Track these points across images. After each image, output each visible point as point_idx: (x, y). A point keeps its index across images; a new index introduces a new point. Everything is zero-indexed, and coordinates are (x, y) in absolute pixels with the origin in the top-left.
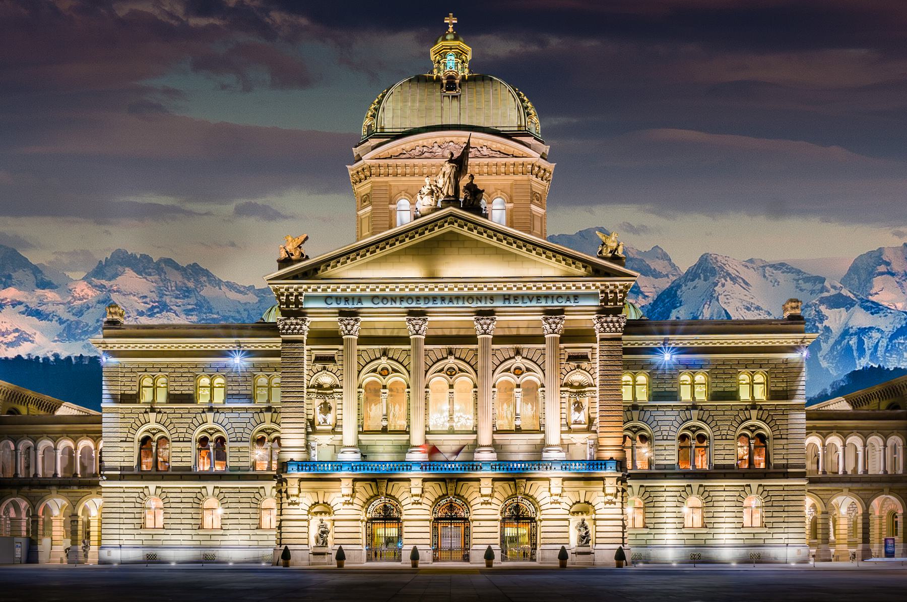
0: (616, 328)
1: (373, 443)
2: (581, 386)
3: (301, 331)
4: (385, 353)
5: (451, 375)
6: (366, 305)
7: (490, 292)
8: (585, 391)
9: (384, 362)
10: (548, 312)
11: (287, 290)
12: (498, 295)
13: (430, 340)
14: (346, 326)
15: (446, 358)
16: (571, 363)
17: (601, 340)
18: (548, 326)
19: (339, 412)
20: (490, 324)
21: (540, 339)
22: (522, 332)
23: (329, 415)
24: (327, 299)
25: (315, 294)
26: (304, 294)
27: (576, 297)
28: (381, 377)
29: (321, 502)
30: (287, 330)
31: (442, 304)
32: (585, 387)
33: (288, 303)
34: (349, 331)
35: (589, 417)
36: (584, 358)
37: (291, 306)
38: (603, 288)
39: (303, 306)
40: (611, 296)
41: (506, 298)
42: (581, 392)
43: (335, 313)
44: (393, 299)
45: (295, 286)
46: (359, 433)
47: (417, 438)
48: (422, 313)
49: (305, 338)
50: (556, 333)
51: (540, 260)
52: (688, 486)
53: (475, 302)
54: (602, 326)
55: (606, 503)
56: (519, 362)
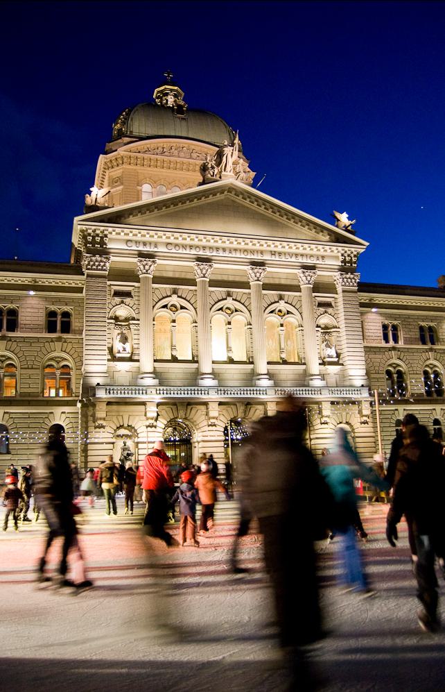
1: (166, 370)
2: (326, 328)
3: (104, 268)
4: (175, 292)
5: (229, 315)
8: (330, 332)
9: (174, 300)
10: (306, 267)
11: (94, 231)
12: (266, 251)
14: (144, 266)
15: (226, 299)
16: (320, 309)
17: (344, 291)
18: (304, 278)
19: (136, 341)
21: (297, 288)
22: (283, 282)
25: (118, 237)
27: (323, 257)
28: (172, 313)
29: (125, 425)
30: (92, 266)
32: (329, 329)
33: (94, 242)
34: (147, 271)
35: (337, 353)
36: (329, 305)
38: (343, 252)
39: (108, 247)
40: (348, 259)
41: (273, 253)
42: (327, 332)
43: (135, 254)
44: (184, 247)
45: (102, 228)
46: (155, 361)
47: (206, 367)
48: (207, 260)
51: (296, 228)
53: (249, 254)
54: (343, 281)
55: (361, 423)
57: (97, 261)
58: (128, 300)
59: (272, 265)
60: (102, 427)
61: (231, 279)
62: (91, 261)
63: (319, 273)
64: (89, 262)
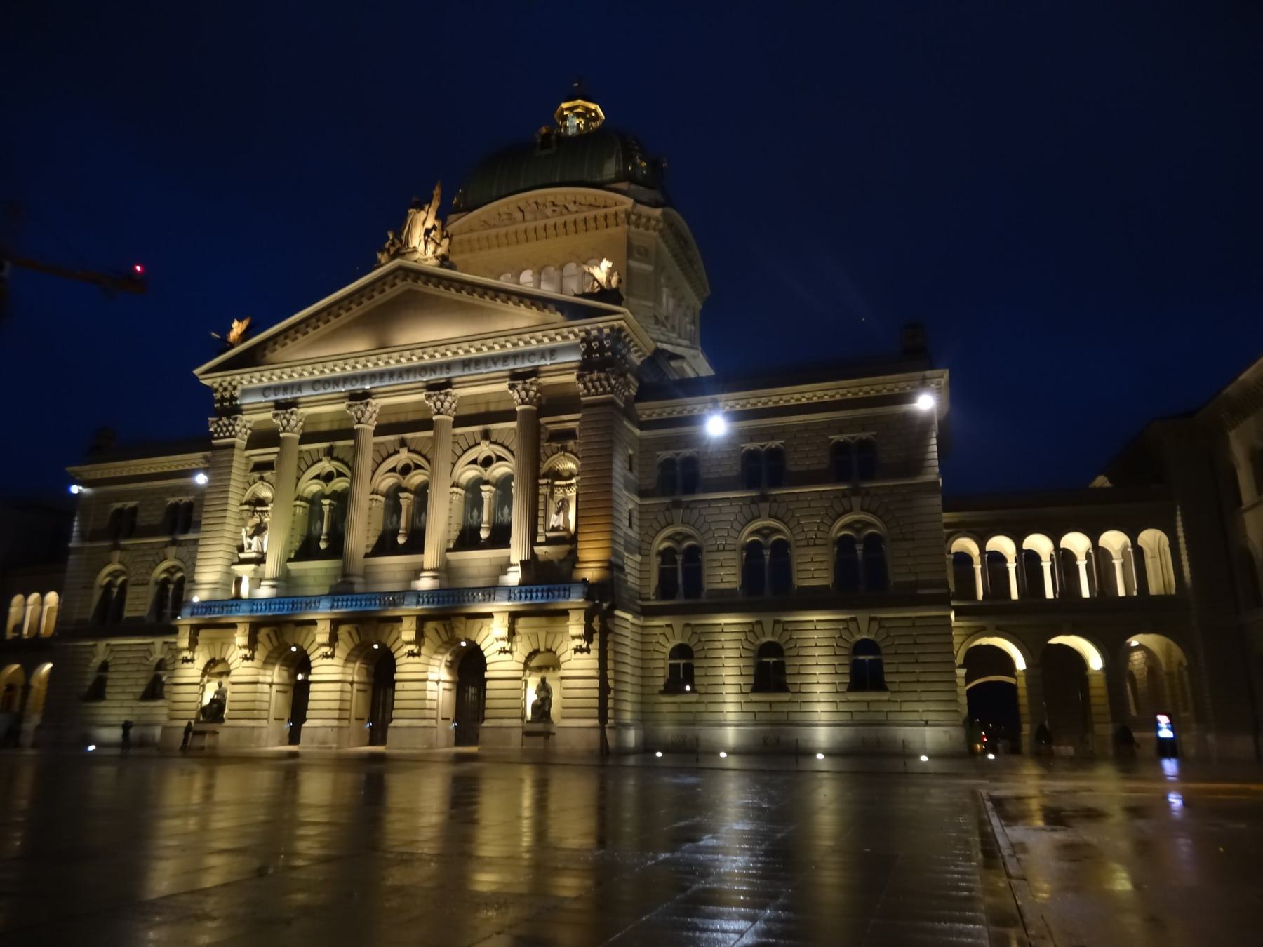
0: (605, 389)
3: (233, 433)
6: (307, 392)
7: (444, 359)
10: (515, 376)
11: (221, 385)
13: (381, 430)
20: (444, 401)
21: (508, 415)
22: (493, 408)
23: (255, 538)
24: (265, 390)
26: (239, 387)
27: (553, 352)
31: (390, 380)
33: (223, 399)
37: (225, 404)
39: (238, 402)
40: (595, 345)
41: (466, 363)
45: (229, 379)
48: (366, 395)
49: (241, 441)
50: (526, 404)
52: (668, 626)
54: (586, 387)
56: (485, 450)
57: (225, 425)
58: (267, 474)
59: (464, 384)
60: (192, 660)
61: (411, 417)
62: (219, 426)
63: (541, 380)
64: (215, 429)
